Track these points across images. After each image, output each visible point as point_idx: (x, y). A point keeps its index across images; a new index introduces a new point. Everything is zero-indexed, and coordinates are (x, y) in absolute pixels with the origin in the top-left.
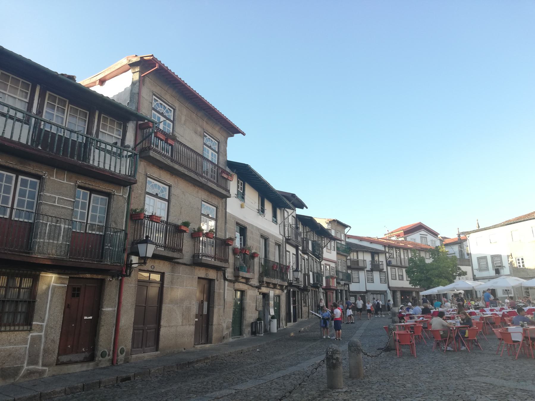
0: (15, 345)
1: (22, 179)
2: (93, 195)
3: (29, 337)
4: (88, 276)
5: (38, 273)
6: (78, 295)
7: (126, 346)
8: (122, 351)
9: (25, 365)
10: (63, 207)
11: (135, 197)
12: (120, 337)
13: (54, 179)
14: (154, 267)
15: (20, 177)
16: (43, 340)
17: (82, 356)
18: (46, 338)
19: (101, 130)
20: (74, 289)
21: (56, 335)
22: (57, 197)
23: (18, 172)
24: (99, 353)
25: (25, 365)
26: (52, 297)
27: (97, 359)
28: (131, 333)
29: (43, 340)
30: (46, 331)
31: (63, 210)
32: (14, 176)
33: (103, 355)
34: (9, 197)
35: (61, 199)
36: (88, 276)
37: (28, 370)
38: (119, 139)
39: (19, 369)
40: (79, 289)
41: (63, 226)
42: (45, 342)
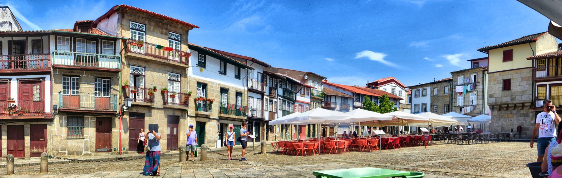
0: (79, 143)
1: (73, 78)
2: (103, 79)
4: (104, 116)
5: (83, 116)
6: (101, 124)
7: (126, 147)
8: (124, 149)
9: (84, 151)
10: (90, 87)
12: (122, 143)
13: (85, 75)
14: (138, 111)
15: (72, 77)
16: (89, 142)
17: (106, 150)
19: (103, 48)
20: (99, 122)
23: (71, 76)
24: (113, 149)
25: (84, 151)
27: (112, 151)
28: (128, 141)
29: (89, 142)
30: (90, 139)
31: (90, 89)
32: (70, 77)
33: (115, 150)
34: (69, 87)
36: (104, 116)
38: (112, 50)
40: (101, 122)
41: (91, 95)
42: (90, 143)
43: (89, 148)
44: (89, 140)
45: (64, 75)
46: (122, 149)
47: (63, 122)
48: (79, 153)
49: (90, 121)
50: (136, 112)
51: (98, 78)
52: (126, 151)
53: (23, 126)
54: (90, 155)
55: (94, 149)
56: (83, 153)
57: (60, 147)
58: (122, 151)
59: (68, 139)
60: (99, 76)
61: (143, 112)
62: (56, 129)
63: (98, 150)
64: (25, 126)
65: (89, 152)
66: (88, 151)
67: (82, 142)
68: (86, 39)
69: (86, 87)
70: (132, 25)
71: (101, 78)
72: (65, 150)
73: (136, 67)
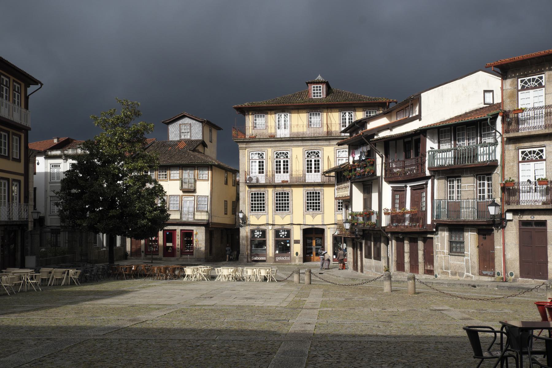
3: (465, 259)
4: (484, 227)
7: (514, 271)
8: (512, 274)
9: (465, 272)
11: (509, 169)
12: (508, 265)
18: (471, 260)
19: (482, 133)
22: (466, 185)
24: (496, 273)
26: (470, 240)
29: (470, 261)
31: (470, 192)
35: (468, 185)
39: (463, 274)
42: (471, 263)
43: (470, 268)
44: (469, 258)
47: (445, 235)
49: (470, 234)
50: (530, 219)
51: (482, 176)
52: (515, 277)
53: (417, 238)
55: (476, 270)
57: (444, 265)
59: (450, 255)
61: (543, 219)
62: (440, 244)
63: (485, 273)
64: (418, 239)
65: (470, 275)
67: (463, 261)
68: (465, 126)
69: (465, 190)
70: (522, 84)
71: (485, 176)
72: (448, 269)
73: (529, 150)
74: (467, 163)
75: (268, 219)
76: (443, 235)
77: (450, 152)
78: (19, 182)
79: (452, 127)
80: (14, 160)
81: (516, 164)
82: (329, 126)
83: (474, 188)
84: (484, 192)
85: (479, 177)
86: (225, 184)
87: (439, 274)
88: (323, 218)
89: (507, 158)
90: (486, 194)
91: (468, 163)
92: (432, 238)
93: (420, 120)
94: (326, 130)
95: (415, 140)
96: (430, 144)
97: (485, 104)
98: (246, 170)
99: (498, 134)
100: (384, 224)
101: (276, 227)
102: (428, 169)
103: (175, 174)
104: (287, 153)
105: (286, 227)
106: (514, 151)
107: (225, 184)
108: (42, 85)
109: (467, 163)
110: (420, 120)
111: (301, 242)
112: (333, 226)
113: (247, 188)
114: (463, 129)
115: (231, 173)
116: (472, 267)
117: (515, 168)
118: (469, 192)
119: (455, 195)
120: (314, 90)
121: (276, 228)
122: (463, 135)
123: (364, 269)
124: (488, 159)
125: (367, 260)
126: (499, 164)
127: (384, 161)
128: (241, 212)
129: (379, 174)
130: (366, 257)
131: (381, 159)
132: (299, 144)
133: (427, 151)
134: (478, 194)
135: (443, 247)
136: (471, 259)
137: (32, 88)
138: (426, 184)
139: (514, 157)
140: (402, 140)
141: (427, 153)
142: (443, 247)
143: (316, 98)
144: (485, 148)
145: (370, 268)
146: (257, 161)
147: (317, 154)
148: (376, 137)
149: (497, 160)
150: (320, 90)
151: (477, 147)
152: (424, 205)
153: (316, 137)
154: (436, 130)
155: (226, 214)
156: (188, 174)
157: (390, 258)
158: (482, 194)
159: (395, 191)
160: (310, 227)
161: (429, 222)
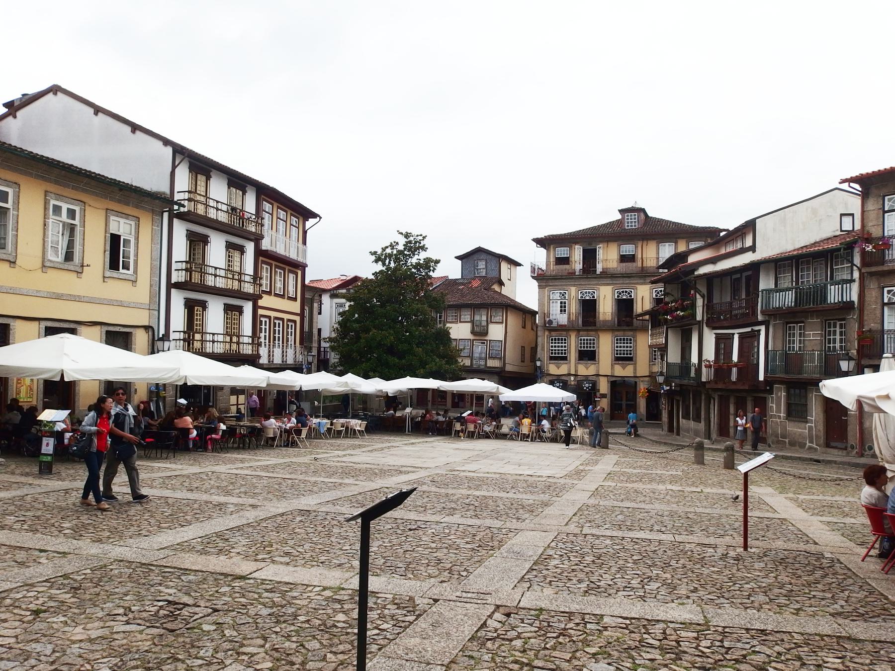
19: (834, 267)
21: (821, 427)
23: (797, 323)
24: (849, 446)
30: (815, 423)
32: (796, 325)
33: (852, 447)
37: (809, 446)
45: (787, 323)
46: (866, 447)
48: (802, 446)
51: (832, 322)
53: (746, 397)
54: (816, 450)
55: (822, 441)
56: (807, 446)
58: (866, 451)
60: (835, 318)
63: (833, 444)
64: (748, 399)
66: (813, 443)
70: (890, 203)
74: (812, 305)
75: (569, 369)
76: (779, 395)
77: (790, 292)
78: (295, 322)
79: (794, 260)
80: (290, 298)
81: (879, 306)
82: (645, 260)
83: (822, 336)
84: (835, 342)
85: (828, 323)
86: (523, 327)
87: (773, 443)
88: (635, 369)
89: (867, 299)
90: (838, 345)
91: (814, 304)
92: (766, 398)
93: (754, 251)
94: (641, 266)
95: (8, 193)
96: (766, 283)
97: (842, 231)
98: (546, 312)
99: (855, 268)
100: (704, 379)
101: (579, 378)
102: (761, 312)
103: (466, 315)
104: (594, 292)
105: (590, 378)
106: (876, 290)
107: (523, 327)
108: (320, 218)
109: (812, 305)
110: (754, 251)
111: (609, 396)
112: (647, 379)
113: (547, 333)
114: (808, 263)
115: (530, 315)
116: (816, 436)
117: (878, 312)
118: (814, 341)
119: (797, 346)
120: (628, 219)
121: (579, 379)
122: (808, 270)
123: (681, 432)
124: (840, 300)
125: (684, 421)
126: (856, 306)
127: (706, 302)
128: (539, 360)
129: (699, 317)
130: (682, 418)
131: (702, 300)
132: (608, 282)
133: (760, 290)
134: (827, 345)
135: (779, 411)
136: (815, 427)
137: (311, 222)
138: (759, 330)
139: (876, 297)
140: (729, 277)
141: (760, 293)
142: (779, 411)
143: (630, 228)
144: (837, 286)
145: (688, 431)
146: (559, 302)
147: (620, 294)
148: (696, 273)
149: (853, 302)
150: (635, 219)
151: (826, 285)
152: (755, 357)
153: (628, 274)
154: (773, 265)
155: (523, 361)
156: (482, 317)
157: (712, 420)
158: (831, 345)
159: (718, 338)
160: (620, 379)
161: (761, 377)
